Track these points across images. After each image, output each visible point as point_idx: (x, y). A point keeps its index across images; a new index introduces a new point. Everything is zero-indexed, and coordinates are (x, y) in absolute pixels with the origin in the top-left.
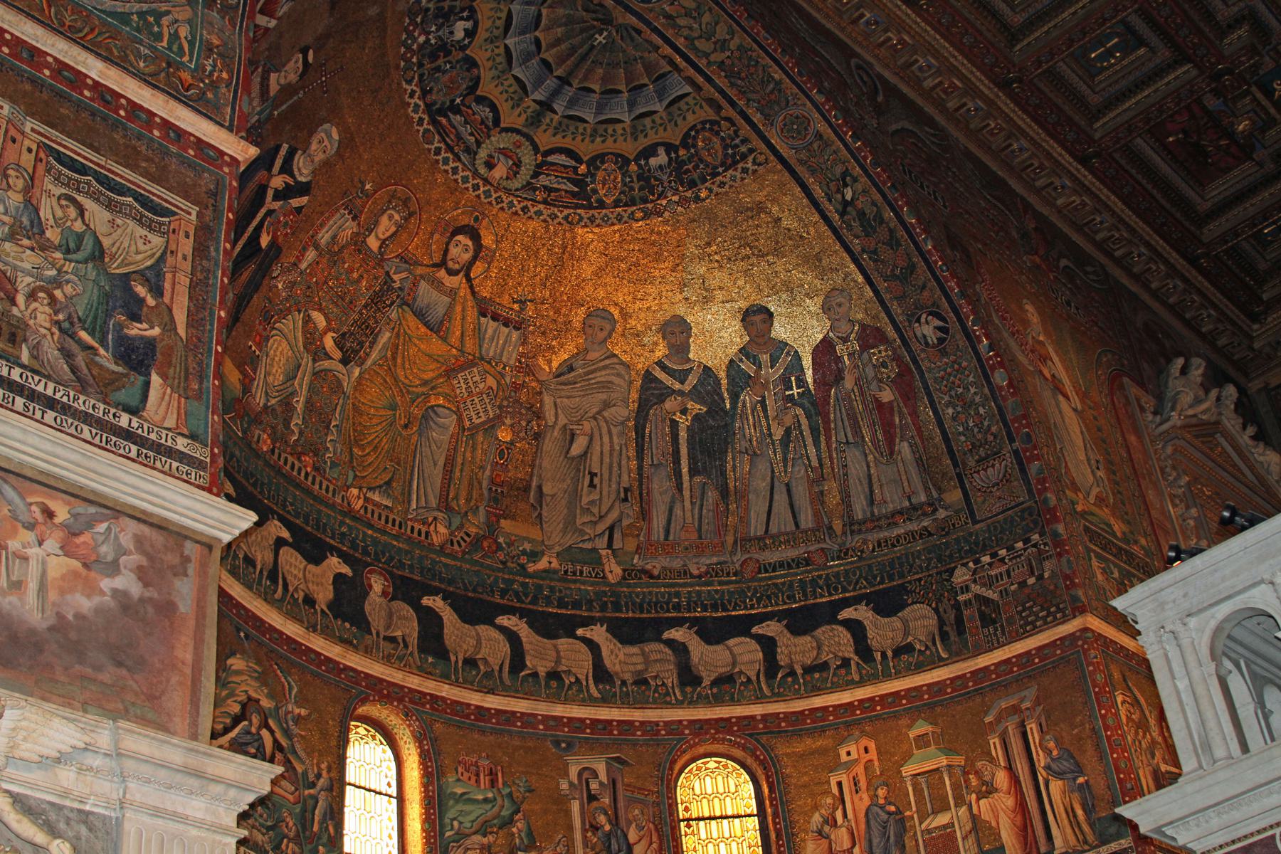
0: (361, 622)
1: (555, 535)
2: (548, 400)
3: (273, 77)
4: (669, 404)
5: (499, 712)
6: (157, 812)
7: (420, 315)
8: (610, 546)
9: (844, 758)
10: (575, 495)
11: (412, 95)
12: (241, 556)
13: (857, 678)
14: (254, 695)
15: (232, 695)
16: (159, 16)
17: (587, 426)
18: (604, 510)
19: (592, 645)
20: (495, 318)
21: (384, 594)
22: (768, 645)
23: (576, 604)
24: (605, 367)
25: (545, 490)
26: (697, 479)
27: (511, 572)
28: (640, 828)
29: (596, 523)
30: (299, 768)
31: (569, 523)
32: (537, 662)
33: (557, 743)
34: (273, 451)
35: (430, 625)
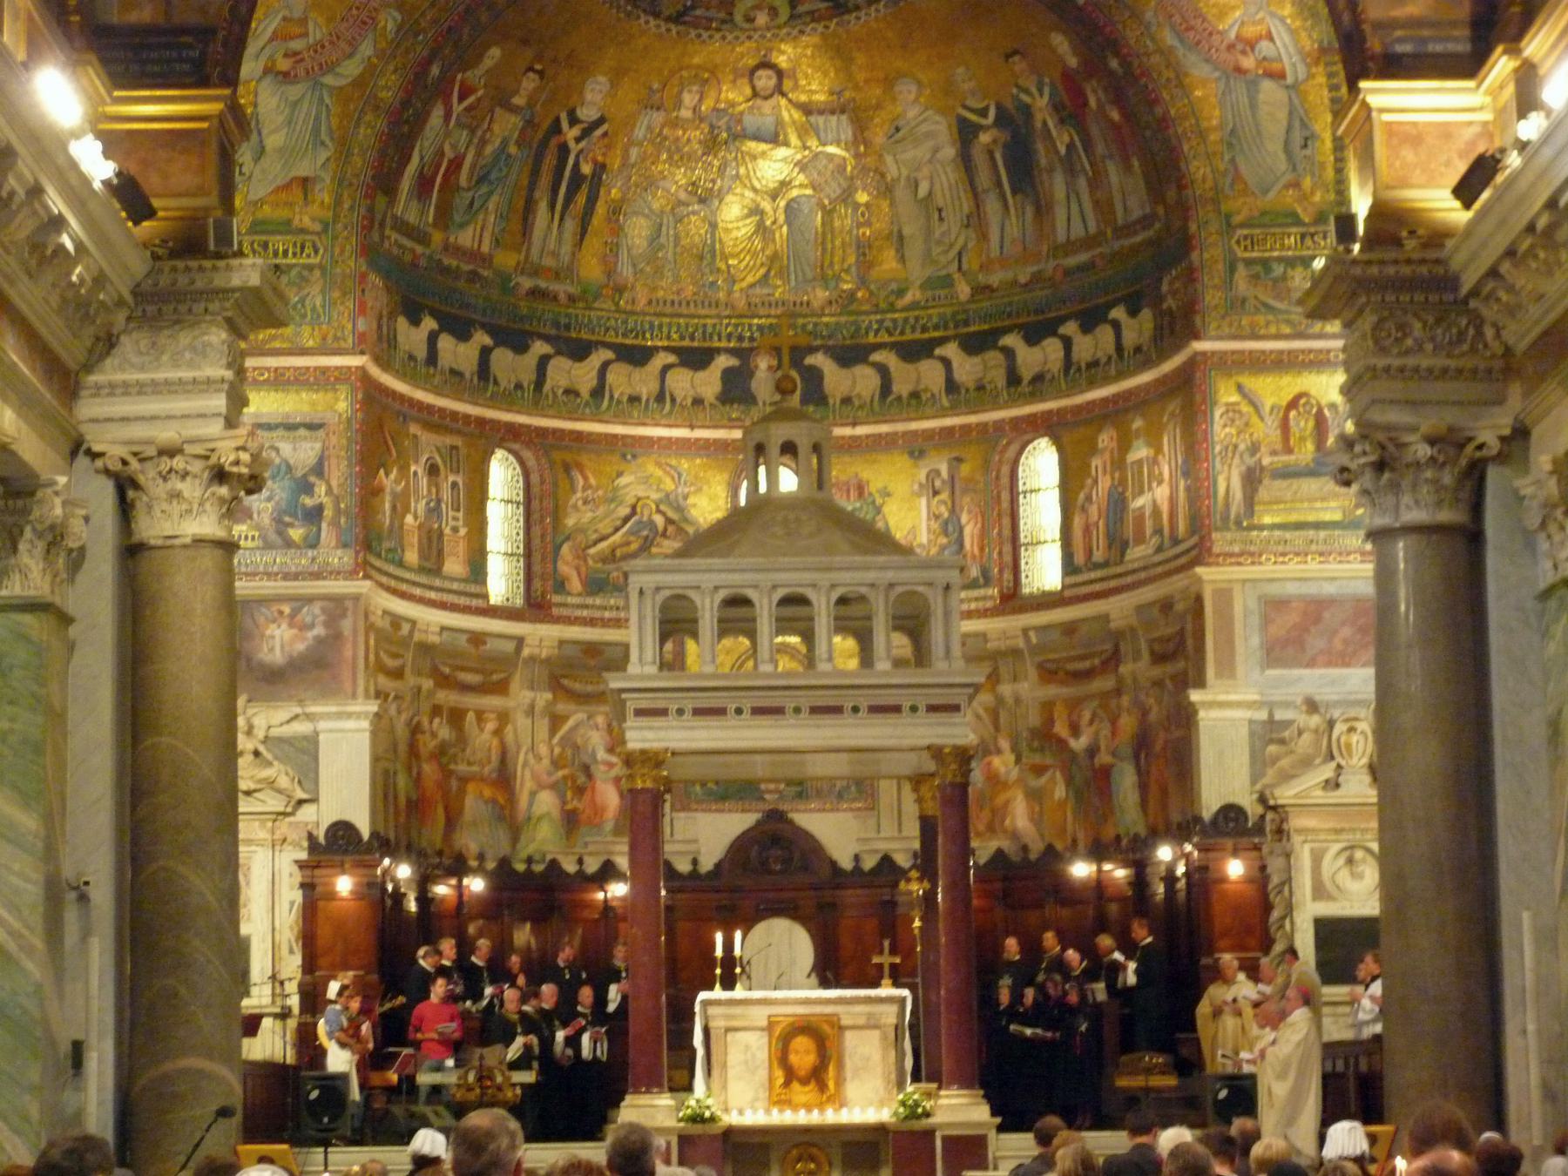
0: (748, 399)
1: (917, 272)
2: (889, 159)
3: (519, 100)
4: (985, 138)
5: (867, 436)
6: (331, 731)
7: (758, 138)
8: (960, 269)
9: (1100, 445)
10: (929, 232)
11: (647, 22)
12: (625, 399)
13: (1113, 372)
14: (641, 494)
15: (621, 503)
16: (302, 301)
17: (925, 171)
18: (953, 237)
19: (946, 363)
20: (821, 112)
21: (770, 368)
22: (1067, 343)
23: (936, 328)
24: (925, 120)
25: (906, 231)
26: (1019, 197)
27: (883, 312)
28: (969, 512)
29: (947, 252)
30: (691, 530)
31: (928, 258)
32: (901, 388)
33: (911, 454)
34: (650, 302)
35: (814, 378)
